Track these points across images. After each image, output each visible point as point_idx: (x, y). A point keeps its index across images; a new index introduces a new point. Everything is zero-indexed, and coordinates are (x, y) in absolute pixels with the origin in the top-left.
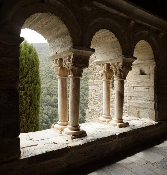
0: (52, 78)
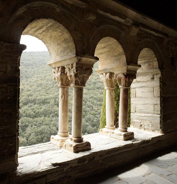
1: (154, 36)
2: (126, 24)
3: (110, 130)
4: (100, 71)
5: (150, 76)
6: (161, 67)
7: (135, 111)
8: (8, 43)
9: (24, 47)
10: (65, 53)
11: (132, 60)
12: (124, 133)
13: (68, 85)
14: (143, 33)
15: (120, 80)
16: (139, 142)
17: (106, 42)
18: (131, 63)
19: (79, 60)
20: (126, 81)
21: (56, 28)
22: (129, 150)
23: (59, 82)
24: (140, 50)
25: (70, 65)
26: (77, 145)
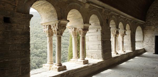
0: (37, 37)
1: (97, 8)
2: (83, 2)
3: (75, 60)
4: (69, 27)
6: (101, 25)
7: (88, 49)
8: (24, 14)
9: (32, 16)
10: (51, 18)
11: (86, 21)
12: (83, 61)
13: (52, 35)
14: (92, 6)
15: (80, 32)
16: (91, 65)
17: (73, 12)
18: (86, 23)
19: (59, 22)
20: (83, 33)
21: (47, 4)
22: (86, 69)
23: (47, 34)
24: (90, 16)
25: (54, 25)
26: (59, 67)
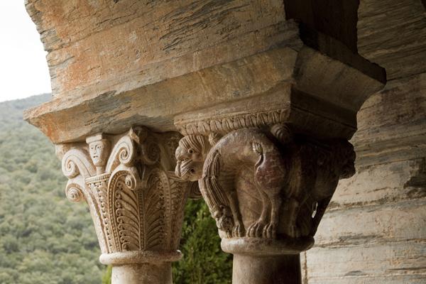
5: (398, 170)
20: (283, 196)
